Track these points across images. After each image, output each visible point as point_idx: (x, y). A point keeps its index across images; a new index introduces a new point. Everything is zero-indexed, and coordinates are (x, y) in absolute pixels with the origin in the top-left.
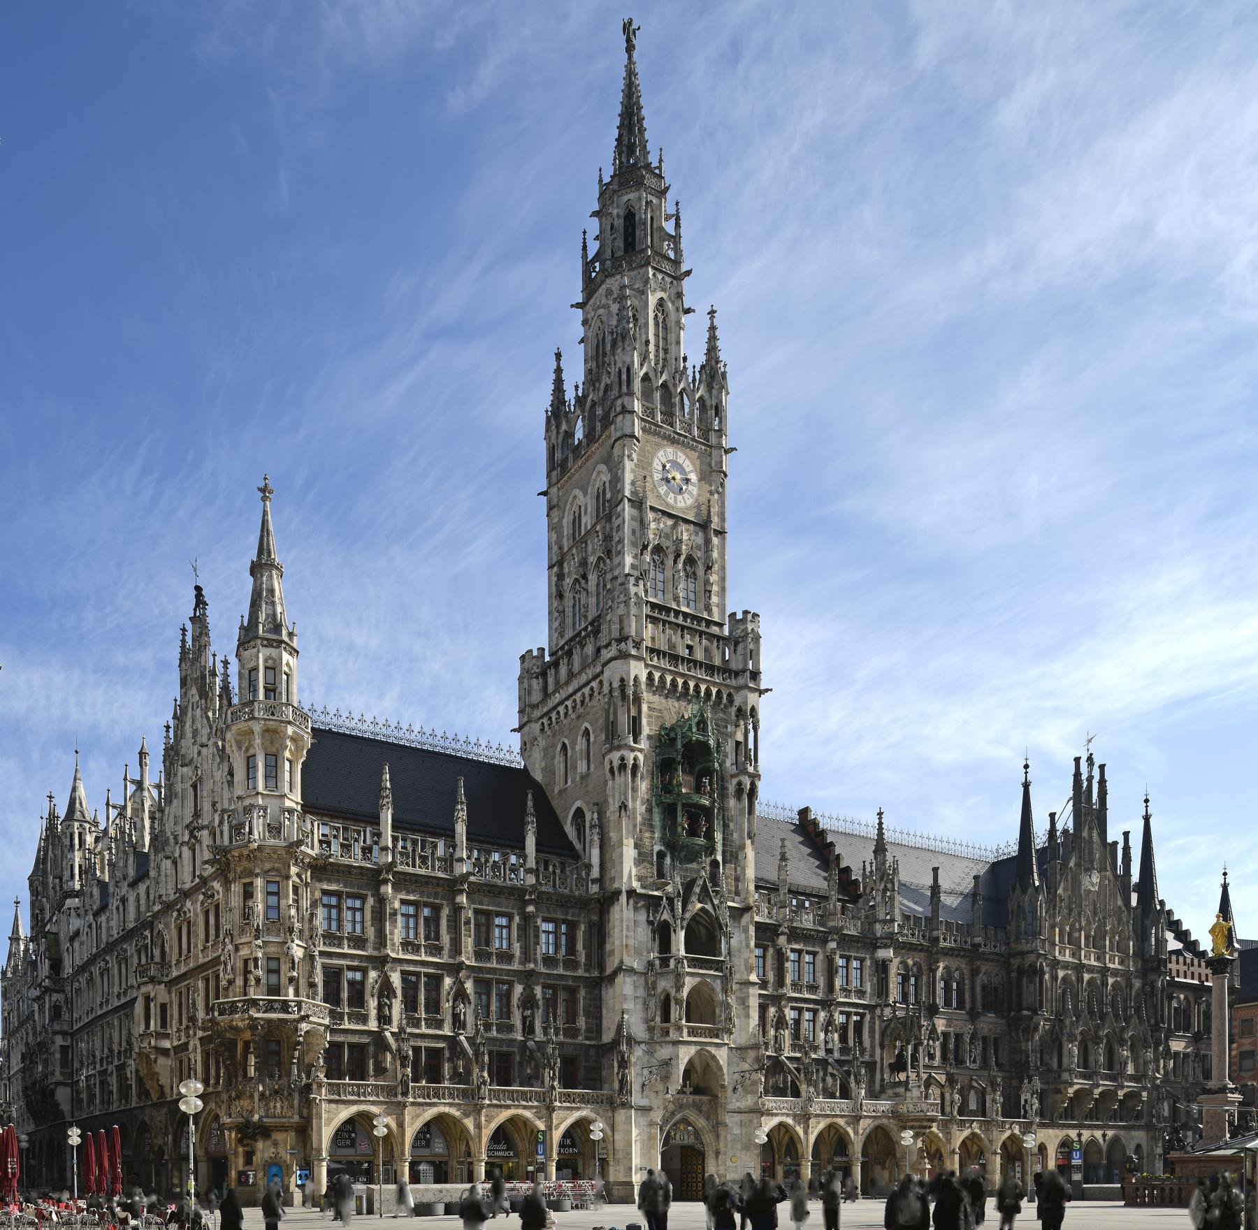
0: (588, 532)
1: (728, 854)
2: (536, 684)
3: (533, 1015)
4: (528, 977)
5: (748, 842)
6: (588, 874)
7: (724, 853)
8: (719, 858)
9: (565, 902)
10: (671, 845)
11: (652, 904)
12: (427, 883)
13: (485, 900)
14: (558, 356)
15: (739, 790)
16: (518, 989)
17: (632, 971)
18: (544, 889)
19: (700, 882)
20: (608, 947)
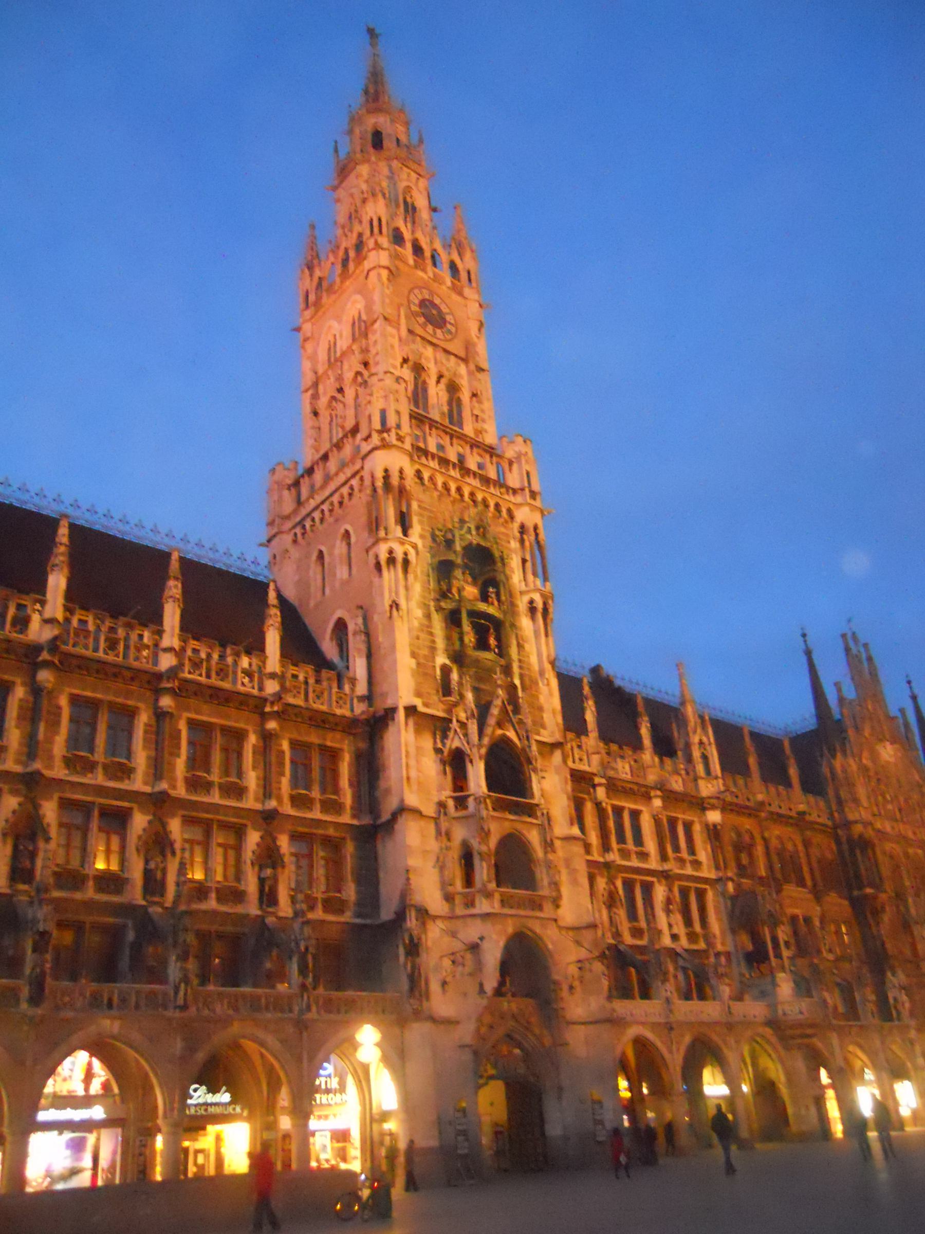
0: (343, 354)
1: (527, 679)
2: (288, 498)
3: (275, 880)
4: (269, 818)
5: (548, 666)
6: (353, 690)
7: (522, 677)
8: (517, 682)
9: (321, 721)
10: (458, 658)
12: (115, 675)
13: (205, 707)
14: (313, 227)
15: (532, 610)
16: (253, 838)
17: (416, 812)
18: (291, 700)
19: (498, 702)
20: (382, 784)
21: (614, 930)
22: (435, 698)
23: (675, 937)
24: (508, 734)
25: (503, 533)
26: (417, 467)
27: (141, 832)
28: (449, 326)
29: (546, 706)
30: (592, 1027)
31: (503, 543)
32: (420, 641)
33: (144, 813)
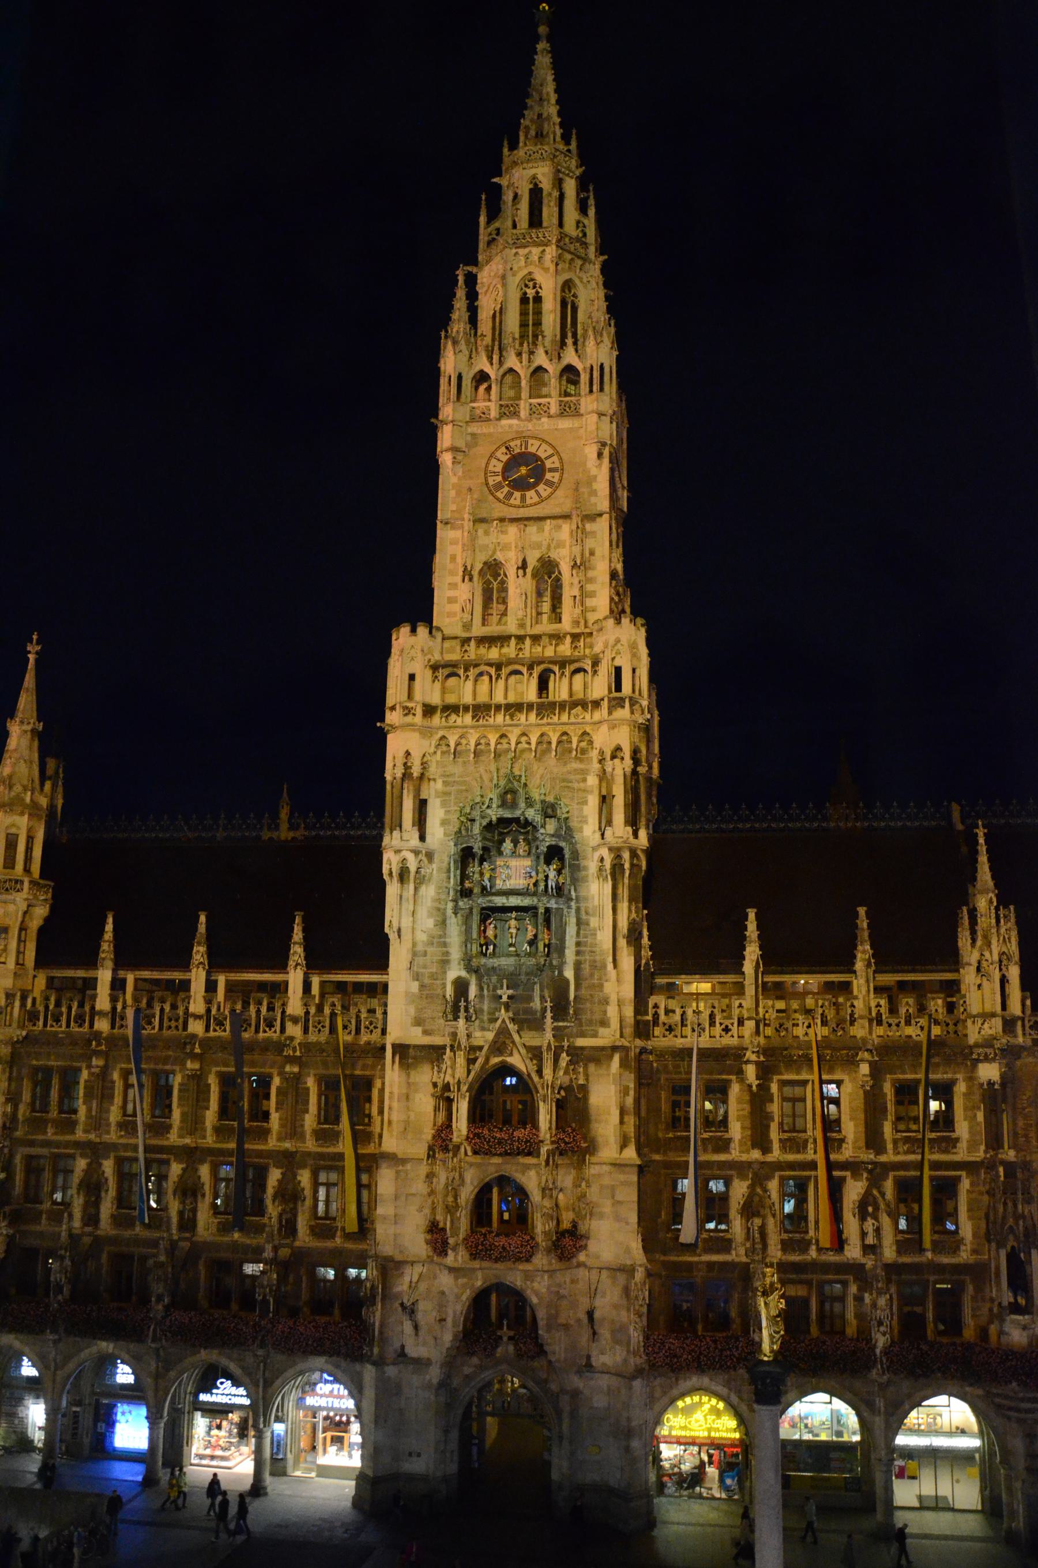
7: (578, 967)
8: (569, 974)
11: (434, 1054)
17: (392, 1158)
21: (748, 1245)
22: (442, 1021)
23: (868, 1249)
24: (509, 1059)
25: (576, 771)
26: (441, 733)
27: (176, 1179)
28: (548, 476)
29: (613, 998)
30: (614, 1378)
31: (576, 785)
32: (428, 957)
33: (180, 1162)
